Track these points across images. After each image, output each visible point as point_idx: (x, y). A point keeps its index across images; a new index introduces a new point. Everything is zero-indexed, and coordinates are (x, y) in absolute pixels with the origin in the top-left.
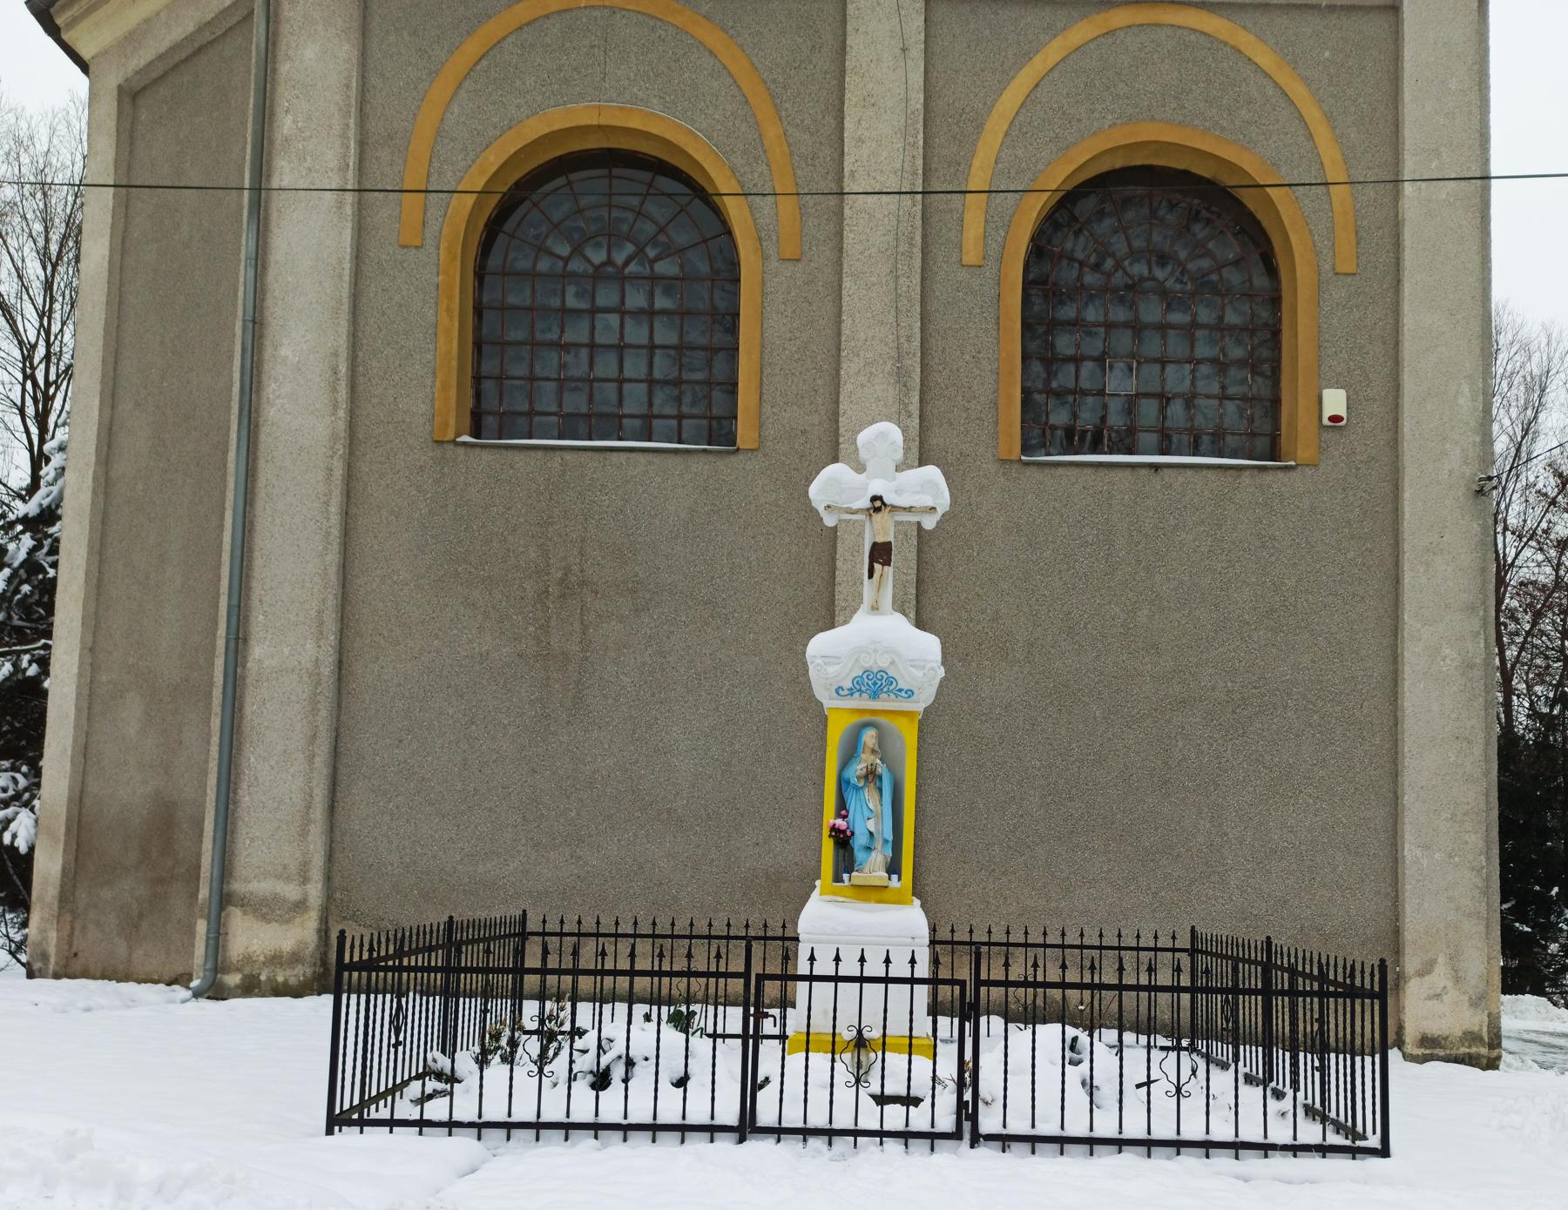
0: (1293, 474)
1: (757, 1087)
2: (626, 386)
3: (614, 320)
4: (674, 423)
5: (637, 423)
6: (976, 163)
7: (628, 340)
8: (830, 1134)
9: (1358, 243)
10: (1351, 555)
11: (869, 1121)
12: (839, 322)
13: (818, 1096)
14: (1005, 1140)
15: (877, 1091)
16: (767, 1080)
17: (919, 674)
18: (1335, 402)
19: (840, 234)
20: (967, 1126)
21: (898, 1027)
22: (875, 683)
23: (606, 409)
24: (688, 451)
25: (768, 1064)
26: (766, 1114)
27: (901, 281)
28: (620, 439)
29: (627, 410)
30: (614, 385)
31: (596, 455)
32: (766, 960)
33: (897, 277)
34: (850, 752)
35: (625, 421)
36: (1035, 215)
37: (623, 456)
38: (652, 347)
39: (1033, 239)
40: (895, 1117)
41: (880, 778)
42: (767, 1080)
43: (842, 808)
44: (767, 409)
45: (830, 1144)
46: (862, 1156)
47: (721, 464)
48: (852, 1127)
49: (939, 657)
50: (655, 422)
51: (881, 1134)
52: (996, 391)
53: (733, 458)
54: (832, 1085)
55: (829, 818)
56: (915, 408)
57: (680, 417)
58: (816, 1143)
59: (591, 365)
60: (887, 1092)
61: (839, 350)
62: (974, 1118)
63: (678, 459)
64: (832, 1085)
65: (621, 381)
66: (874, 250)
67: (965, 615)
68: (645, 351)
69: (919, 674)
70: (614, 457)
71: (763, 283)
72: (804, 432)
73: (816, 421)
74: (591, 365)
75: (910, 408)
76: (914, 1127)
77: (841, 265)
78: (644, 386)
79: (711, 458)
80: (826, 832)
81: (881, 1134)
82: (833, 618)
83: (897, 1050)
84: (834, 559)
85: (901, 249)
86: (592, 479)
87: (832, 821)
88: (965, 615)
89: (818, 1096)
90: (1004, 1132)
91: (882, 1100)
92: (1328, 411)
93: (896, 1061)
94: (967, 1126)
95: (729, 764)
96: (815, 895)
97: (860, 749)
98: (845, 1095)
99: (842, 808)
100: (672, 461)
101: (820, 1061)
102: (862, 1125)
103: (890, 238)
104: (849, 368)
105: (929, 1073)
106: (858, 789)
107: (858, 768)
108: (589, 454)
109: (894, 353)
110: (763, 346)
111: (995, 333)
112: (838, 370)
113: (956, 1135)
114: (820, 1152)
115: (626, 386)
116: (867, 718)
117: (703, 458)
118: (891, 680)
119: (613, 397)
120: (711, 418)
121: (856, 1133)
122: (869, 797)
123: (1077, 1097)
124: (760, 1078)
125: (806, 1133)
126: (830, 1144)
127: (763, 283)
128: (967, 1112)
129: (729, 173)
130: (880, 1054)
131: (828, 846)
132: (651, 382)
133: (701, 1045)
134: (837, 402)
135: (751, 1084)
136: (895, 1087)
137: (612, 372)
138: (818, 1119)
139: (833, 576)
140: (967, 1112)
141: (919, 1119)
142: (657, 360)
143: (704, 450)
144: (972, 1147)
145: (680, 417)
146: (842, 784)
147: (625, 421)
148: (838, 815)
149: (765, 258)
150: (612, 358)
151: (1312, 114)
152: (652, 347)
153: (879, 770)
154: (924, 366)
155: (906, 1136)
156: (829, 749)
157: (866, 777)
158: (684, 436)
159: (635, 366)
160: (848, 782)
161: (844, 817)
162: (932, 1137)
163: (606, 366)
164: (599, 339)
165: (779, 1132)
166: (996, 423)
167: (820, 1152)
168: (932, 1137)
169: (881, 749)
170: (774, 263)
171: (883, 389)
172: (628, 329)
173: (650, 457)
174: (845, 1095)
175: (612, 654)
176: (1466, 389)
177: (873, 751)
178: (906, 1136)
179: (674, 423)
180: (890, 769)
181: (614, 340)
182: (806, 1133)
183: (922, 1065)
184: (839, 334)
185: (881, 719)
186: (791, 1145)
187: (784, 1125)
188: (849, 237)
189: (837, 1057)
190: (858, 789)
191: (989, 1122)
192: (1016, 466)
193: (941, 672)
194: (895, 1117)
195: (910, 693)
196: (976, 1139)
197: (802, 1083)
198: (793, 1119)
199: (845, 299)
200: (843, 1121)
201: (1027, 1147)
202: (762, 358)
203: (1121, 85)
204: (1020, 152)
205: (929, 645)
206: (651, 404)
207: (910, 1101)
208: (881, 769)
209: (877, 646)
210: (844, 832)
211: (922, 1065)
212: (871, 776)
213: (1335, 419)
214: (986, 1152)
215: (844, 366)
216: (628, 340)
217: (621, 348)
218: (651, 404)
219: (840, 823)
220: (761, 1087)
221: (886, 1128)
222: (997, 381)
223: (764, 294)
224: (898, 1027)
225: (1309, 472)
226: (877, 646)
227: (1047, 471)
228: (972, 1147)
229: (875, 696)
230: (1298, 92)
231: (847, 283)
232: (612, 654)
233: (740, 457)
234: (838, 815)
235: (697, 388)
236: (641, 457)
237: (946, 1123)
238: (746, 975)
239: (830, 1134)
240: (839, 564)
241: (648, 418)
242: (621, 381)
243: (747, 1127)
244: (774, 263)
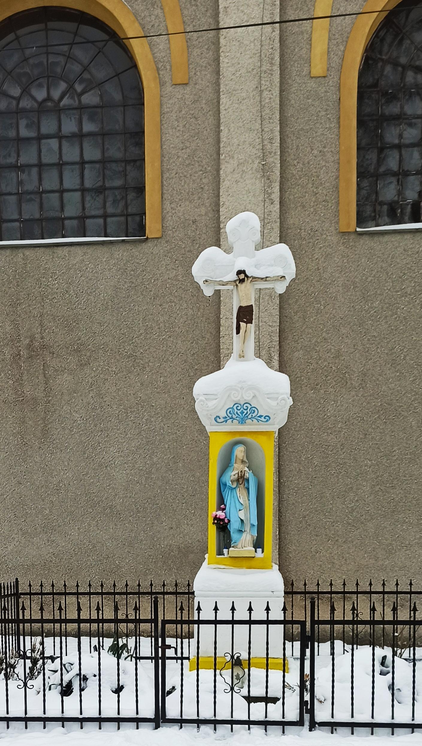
1: (166, 694)
2: (66, 195)
3: (54, 143)
4: (101, 221)
5: (75, 222)
7: (65, 158)
8: (215, 723)
11: (241, 714)
12: (218, 132)
13: (206, 698)
14: (333, 726)
15: (246, 694)
16: (174, 688)
17: (274, 403)
19: (217, 60)
20: (307, 717)
21: (258, 651)
22: (243, 412)
23: (52, 214)
24: (111, 242)
25: (172, 678)
26: (172, 709)
27: (265, 93)
28: (63, 237)
29: (67, 214)
30: (57, 195)
31: (48, 251)
32: (169, 611)
33: (261, 92)
34: (226, 464)
35: (67, 222)
36: (367, 30)
37: (66, 249)
38: (82, 163)
39: (366, 50)
40: (258, 711)
41: (248, 480)
42: (174, 688)
43: (221, 503)
44: (167, 206)
45: (215, 729)
46: (236, 736)
47: (135, 251)
48: (229, 718)
49: (289, 391)
50: (88, 222)
51: (249, 723)
52: (338, 177)
54: (215, 692)
55: (213, 511)
56: (276, 196)
57: (105, 216)
58: (206, 729)
59: (40, 179)
60: (253, 694)
61: (219, 154)
62: (311, 712)
63: (105, 249)
64: (215, 692)
65: (62, 191)
66: (243, 71)
67: (315, 355)
68: (77, 166)
69: (274, 403)
70: (60, 251)
71: (161, 105)
73: (203, 212)
74: (40, 179)
75: (273, 196)
76: (271, 718)
77: (219, 85)
78: (78, 194)
79: (128, 246)
80: (211, 520)
81: (249, 723)
82: (219, 362)
83: (258, 666)
84: (219, 318)
85: (264, 68)
86: (45, 269)
87: (214, 513)
88: (315, 355)
89: (206, 698)
90: (332, 721)
91: (250, 699)
93: (257, 674)
94: (307, 717)
95: (150, 472)
96: (205, 564)
97: (233, 460)
98: (224, 698)
99: (221, 503)
100: (99, 251)
101: (207, 675)
102: (236, 717)
103: (256, 59)
104: (226, 168)
105: (283, 681)
106: (232, 489)
107: (232, 474)
108: (42, 249)
109: (260, 154)
110: (163, 156)
111: (336, 130)
112: (218, 170)
113: (300, 723)
114: (209, 734)
115: (66, 195)
116: (238, 438)
117: (123, 247)
118: (253, 409)
119: (56, 203)
120: (127, 215)
121: (232, 722)
122: (240, 494)
123: (383, 695)
124: (167, 689)
125: (199, 722)
126: (215, 729)
127: (161, 105)
128: (307, 708)
129: (132, 18)
130: (246, 670)
131: (212, 530)
132: (83, 190)
133: (127, 665)
134: (218, 196)
135: (161, 692)
136: (258, 691)
137: (55, 185)
138: (206, 713)
139: (219, 332)
140: (307, 708)
141: (274, 712)
142: (87, 172)
143: (123, 240)
144: (310, 730)
145: (105, 216)
146: (221, 486)
147: (67, 222)
148: (219, 509)
149: (162, 84)
150: (54, 173)
152: (82, 163)
153: (247, 475)
154: (283, 162)
155: (265, 724)
156: (211, 461)
157: (238, 480)
158: (108, 231)
159: (71, 180)
160: (225, 485)
161: (223, 509)
162: (283, 724)
163: (51, 181)
164: (45, 160)
165: (181, 722)
166: (338, 203)
167: (209, 734)
168: (283, 724)
169: (249, 460)
170: (169, 89)
171: (253, 184)
172: (64, 151)
173: (85, 249)
174: (224, 698)
175: (66, 398)
177: (243, 461)
178: (265, 724)
179: (101, 221)
180: (255, 474)
181: (54, 159)
182: (199, 722)
183: (276, 675)
184: (218, 141)
185: (248, 438)
186: (189, 730)
187: (184, 717)
188: (224, 61)
189: (218, 672)
190: (232, 489)
191: (322, 714)
193: (290, 402)
194: (258, 711)
195: (268, 418)
196: (313, 725)
197: (196, 689)
198: (190, 713)
199: (223, 112)
200: (223, 714)
201: (348, 730)
202: (162, 166)
205: (282, 382)
206: (84, 208)
207: (267, 700)
208: (249, 474)
209: (246, 385)
210: (223, 520)
211: (276, 675)
212: (241, 479)
214: (320, 734)
215: (223, 167)
216: (65, 158)
217: (60, 165)
218: (84, 208)
219: (220, 514)
220: (170, 693)
221: (252, 719)
222: (338, 170)
223: (162, 114)
224: (258, 651)
226: (246, 385)
228: (310, 730)
229: (242, 422)
231: (224, 100)
232: (66, 398)
234: (219, 509)
235: (117, 192)
236: (79, 250)
237: (293, 715)
238: (155, 621)
239: (215, 723)
240: (222, 322)
241: (82, 218)
242: (62, 191)
243: (160, 719)
244: (169, 89)
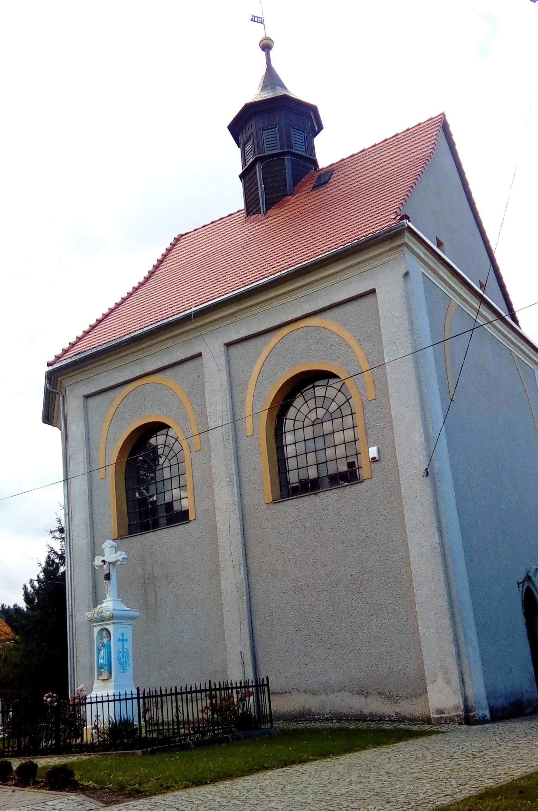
0: (363, 484)
6: (248, 399)
9: (375, 386)
10: (388, 511)
18: (373, 452)
53: (189, 524)
72: (208, 510)
92: (371, 457)
151: (352, 342)
176: (417, 434)
192: (271, 504)
203: (289, 355)
204: (261, 391)
213: (374, 458)
225: (369, 481)
227: (281, 503)
230: (346, 335)
233: (191, 523)
